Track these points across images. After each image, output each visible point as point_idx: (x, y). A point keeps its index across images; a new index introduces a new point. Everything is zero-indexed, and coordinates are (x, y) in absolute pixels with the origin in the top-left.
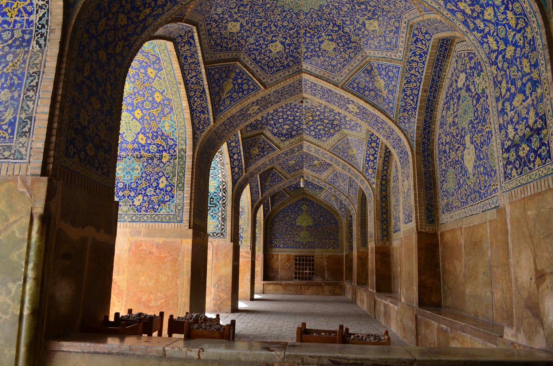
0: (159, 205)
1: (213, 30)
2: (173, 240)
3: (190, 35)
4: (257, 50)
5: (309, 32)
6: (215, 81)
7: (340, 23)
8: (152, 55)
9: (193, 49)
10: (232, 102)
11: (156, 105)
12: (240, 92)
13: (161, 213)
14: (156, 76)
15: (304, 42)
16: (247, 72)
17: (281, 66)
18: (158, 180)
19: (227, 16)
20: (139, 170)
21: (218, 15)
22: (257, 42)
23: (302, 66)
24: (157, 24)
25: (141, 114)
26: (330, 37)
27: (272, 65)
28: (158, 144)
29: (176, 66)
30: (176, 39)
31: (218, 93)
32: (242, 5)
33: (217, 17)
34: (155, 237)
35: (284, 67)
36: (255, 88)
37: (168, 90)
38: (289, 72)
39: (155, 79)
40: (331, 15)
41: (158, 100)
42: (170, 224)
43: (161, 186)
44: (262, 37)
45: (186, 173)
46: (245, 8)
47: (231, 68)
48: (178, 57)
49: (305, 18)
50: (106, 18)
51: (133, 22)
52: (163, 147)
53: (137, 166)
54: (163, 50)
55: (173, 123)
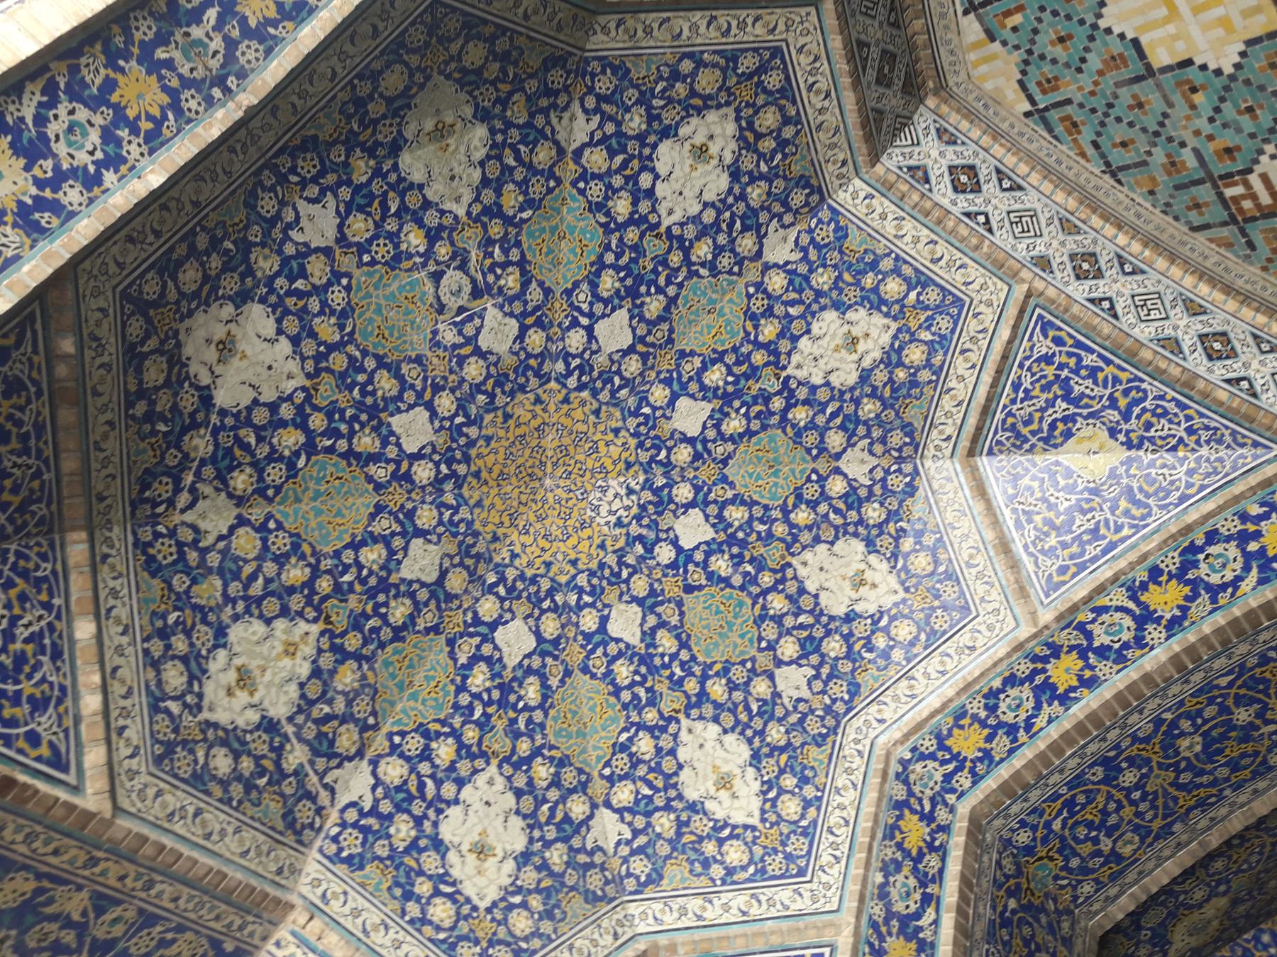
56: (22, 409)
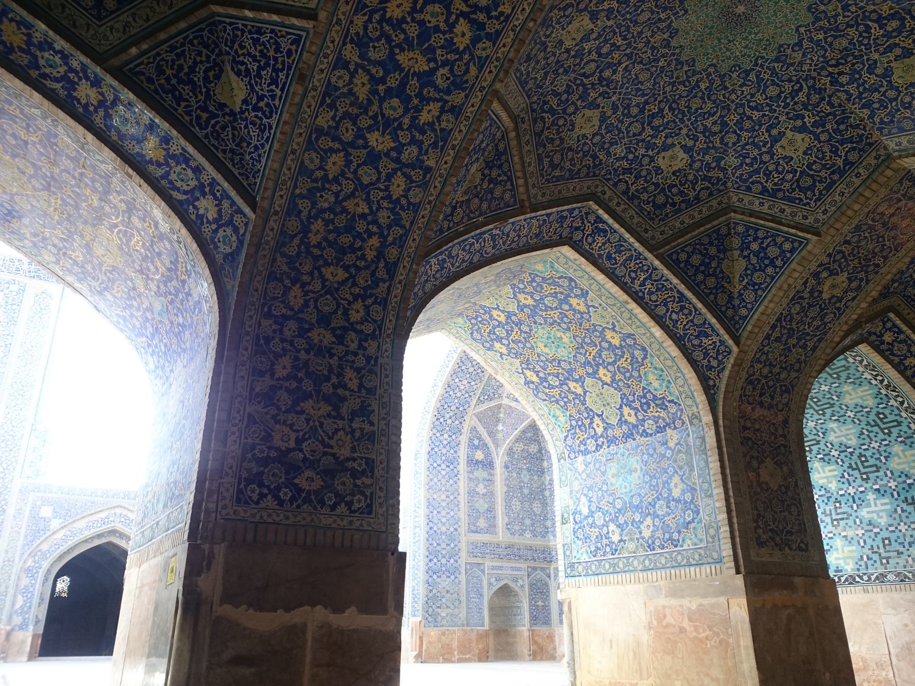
0: (679, 532)
1: (633, 189)
2: (713, 600)
3: (592, 218)
4: (757, 171)
5: (841, 73)
6: (697, 269)
7: (891, 8)
8: (559, 278)
9: (614, 238)
10: (760, 293)
11: (619, 352)
12: (766, 266)
13: (685, 547)
14: (588, 307)
15: (849, 100)
16: (762, 222)
17: (833, 173)
18: (669, 484)
19: (642, 151)
20: (639, 471)
21: (623, 158)
22: (745, 158)
23: (885, 148)
24: (411, 250)
25: (609, 375)
26: (898, 51)
27: (809, 182)
28: (654, 417)
29: (601, 277)
30: (571, 238)
31: (719, 287)
32: (653, 116)
33: (625, 164)
34: (682, 597)
35: (842, 172)
36: (796, 245)
37: (618, 321)
38: (858, 175)
39: (589, 312)
40: (853, 9)
41: (616, 342)
42: (703, 567)
43: (676, 493)
44: (747, 144)
45: (710, 460)
46: (663, 117)
47: (724, 231)
48: (595, 263)
49: (804, 55)
50: (298, 285)
51: (359, 269)
52: (664, 419)
53: (635, 465)
54: (566, 263)
55: (660, 373)
56: (167, 61)
